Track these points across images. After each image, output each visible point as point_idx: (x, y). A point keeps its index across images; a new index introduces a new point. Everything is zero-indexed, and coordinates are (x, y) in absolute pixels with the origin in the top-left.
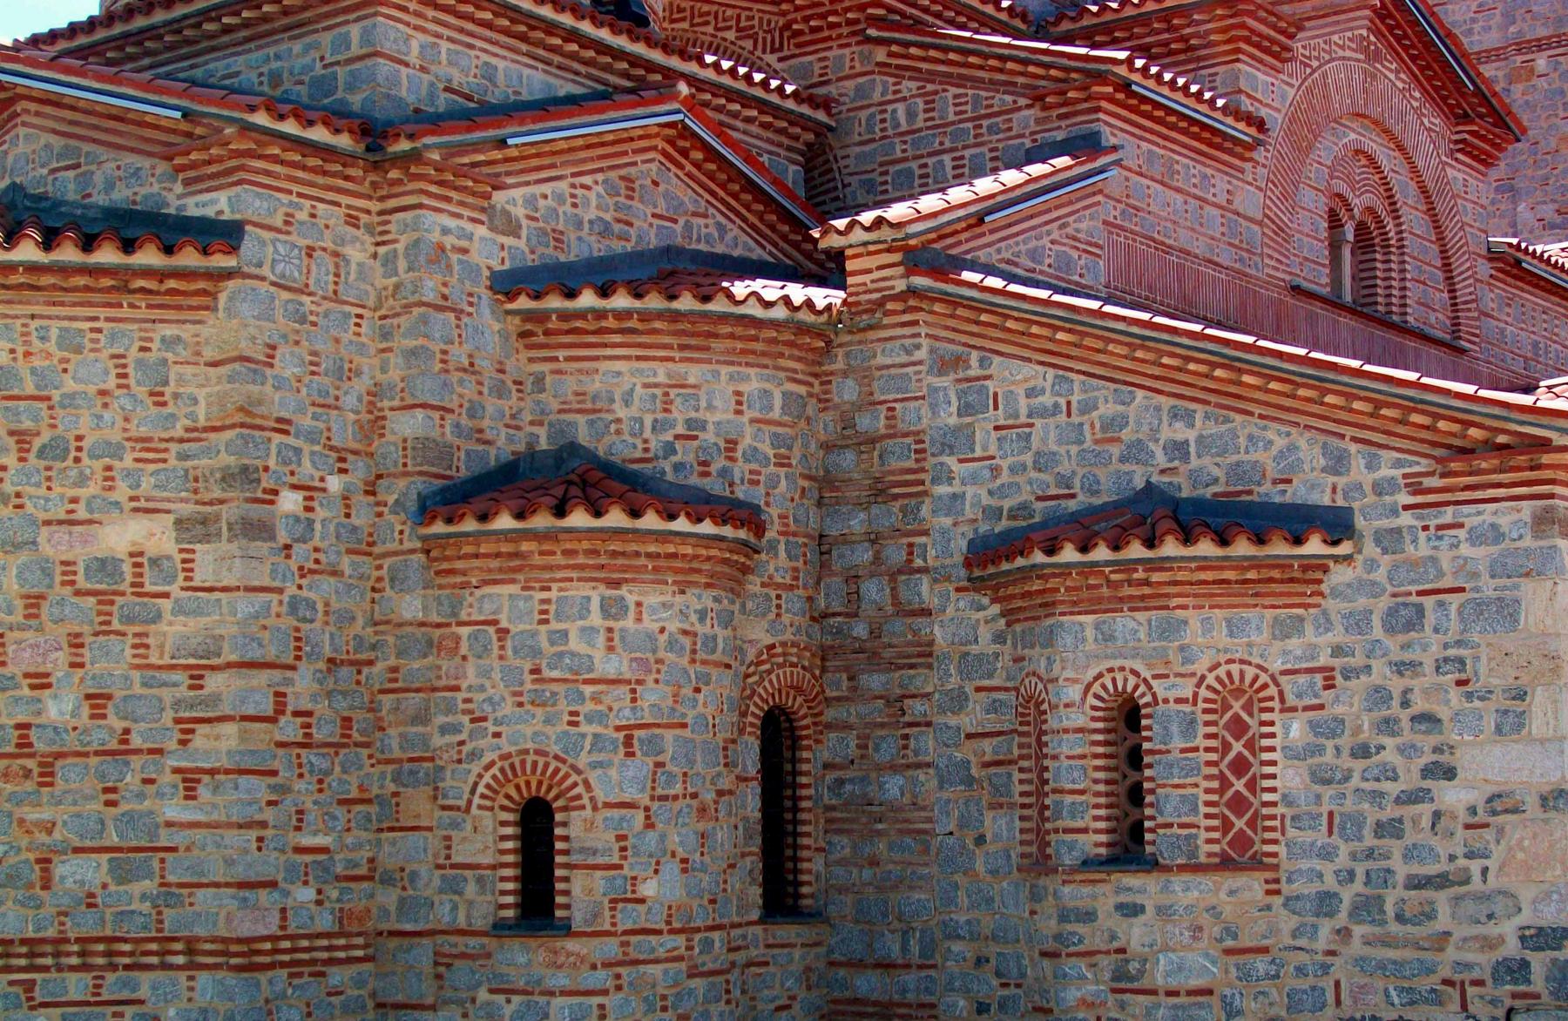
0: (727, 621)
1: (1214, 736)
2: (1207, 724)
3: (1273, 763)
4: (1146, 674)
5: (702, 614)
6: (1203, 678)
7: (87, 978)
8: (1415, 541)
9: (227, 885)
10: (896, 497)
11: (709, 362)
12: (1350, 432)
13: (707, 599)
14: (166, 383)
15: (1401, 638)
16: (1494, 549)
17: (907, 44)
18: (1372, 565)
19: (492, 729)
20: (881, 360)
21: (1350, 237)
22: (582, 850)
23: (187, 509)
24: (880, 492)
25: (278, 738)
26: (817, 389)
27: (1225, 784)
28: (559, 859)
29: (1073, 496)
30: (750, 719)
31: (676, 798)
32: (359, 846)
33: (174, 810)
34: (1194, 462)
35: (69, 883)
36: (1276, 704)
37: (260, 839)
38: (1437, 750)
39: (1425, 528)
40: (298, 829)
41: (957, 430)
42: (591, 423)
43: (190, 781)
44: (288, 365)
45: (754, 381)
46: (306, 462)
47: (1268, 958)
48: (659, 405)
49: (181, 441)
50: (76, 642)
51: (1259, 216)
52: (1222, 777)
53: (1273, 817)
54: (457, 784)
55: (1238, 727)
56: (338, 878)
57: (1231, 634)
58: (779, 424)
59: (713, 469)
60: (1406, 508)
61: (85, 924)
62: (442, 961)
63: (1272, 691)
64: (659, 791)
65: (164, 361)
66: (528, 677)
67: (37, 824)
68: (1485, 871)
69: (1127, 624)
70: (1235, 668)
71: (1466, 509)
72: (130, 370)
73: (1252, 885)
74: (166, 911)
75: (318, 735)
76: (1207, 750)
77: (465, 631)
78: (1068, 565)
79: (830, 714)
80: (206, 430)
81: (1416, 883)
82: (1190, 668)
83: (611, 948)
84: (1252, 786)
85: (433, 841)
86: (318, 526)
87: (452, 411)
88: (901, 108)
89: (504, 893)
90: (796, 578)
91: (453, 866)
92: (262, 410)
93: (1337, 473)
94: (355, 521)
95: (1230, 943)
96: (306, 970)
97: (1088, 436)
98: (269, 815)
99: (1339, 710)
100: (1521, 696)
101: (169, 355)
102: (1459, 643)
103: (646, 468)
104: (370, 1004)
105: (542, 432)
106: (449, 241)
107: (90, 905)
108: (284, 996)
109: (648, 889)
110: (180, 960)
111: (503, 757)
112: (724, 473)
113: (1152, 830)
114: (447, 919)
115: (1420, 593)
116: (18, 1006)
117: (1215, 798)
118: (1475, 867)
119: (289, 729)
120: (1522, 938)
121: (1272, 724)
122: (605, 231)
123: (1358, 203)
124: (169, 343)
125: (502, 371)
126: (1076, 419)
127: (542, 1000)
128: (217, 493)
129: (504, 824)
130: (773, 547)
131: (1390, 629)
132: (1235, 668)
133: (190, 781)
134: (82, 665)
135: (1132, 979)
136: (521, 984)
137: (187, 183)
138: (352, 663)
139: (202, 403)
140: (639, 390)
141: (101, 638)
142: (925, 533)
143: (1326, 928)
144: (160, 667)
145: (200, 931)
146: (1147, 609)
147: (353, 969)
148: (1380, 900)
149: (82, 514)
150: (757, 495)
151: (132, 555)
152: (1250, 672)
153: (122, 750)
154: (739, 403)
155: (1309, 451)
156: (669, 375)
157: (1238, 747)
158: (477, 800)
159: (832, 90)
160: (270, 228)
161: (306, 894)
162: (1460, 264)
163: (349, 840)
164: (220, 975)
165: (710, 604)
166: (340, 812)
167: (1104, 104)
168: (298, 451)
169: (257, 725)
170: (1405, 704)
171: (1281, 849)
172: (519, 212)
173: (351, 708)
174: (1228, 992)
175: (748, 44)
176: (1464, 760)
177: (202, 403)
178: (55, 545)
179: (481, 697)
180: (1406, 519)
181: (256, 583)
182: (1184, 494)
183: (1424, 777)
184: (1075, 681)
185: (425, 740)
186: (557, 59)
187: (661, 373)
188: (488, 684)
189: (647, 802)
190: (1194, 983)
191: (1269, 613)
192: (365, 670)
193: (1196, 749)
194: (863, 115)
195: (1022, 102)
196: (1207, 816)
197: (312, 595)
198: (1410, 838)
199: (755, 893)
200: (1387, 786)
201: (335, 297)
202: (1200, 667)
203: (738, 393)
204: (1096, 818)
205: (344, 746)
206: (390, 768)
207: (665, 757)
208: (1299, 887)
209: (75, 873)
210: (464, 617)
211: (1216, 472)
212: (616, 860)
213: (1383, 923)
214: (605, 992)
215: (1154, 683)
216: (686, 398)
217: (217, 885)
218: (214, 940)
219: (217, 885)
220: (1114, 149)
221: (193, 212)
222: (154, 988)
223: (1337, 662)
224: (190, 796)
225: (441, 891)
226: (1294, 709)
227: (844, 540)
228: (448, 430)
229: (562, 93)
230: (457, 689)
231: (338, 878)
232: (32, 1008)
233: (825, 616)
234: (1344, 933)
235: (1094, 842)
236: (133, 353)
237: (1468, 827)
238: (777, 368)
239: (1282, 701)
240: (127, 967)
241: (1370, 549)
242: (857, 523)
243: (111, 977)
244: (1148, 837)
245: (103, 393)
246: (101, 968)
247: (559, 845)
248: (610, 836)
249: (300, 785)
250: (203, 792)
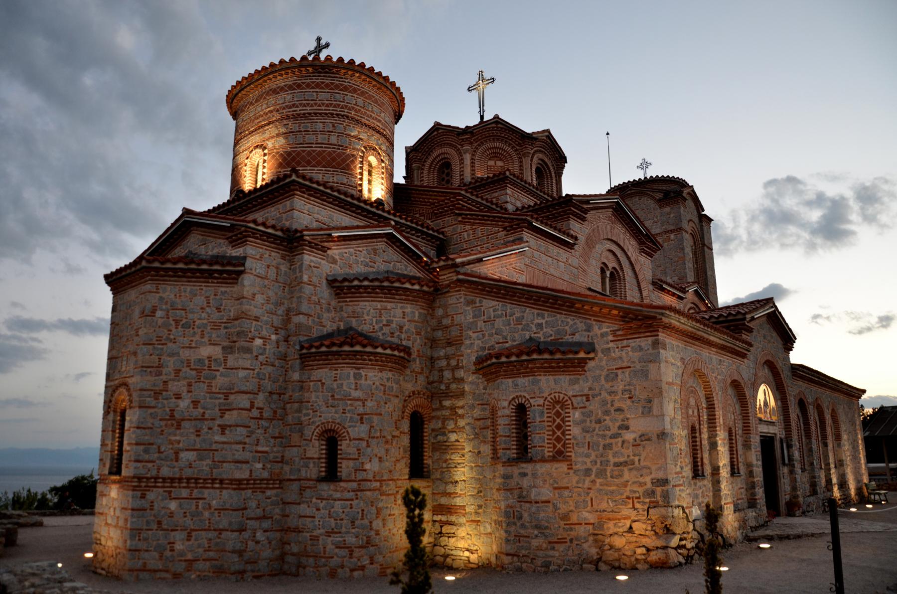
0: (398, 382)
1: (550, 417)
2: (548, 413)
3: (570, 426)
4: (528, 397)
5: (388, 379)
6: (546, 398)
7: (188, 491)
8: (614, 352)
9: (232, 462)
10: (454, 345)
11: (394, 302)
12: (593, 318)
13: (390, 374)
14: (221, 305)
15: (610, 384)
16: (640, 354)
17: (466, 215)
18: (601, 360)
19: (319, 414)
20: (450, 302)
21: (608, 275)
22: (345, 453)
23: (226, 344)
24: (450, 344)
25: (251, 416)
26: (431, 311)
27: (554, 433)
28: (339, 456)
29: (507, 342)
30: (406, 414)
31: (377, 437)
32: (278, 452)
33: (218, 438)
34: (545, 330)
35: (184, 460)
36: (570, 406)
37: (244, 448)
38: (623, 421)
39: (618, 348)
40: (257, 445)
41: (473, 322)
42: (357, 321)
43: (223, 428)
44: (260, 299)
45: (409, 309)
46: (264, 330)
47: (568, 491)
48: (378, 316)
49: (225, 323)
50: (190, 385)
51: (577, 266)
52: (553, 431)
53: (570, 444)
54: (308, 432)
55: (558, 414)
56: (270, 461)
57: (555, 384)
58: (417, 322)
59: (395, 335)
60: (611, 341)
61: (188, 473)
62: (302, 489)
63: (569, 402)
64: (372, 435)
65: (221, 299)
66: (330, 398)
67: (175, 441)
68: (639, 460)
69: (522, 381)
70: (557, 395)
71: (630, 341)
72: (211, 301)
73: (563, 467)
74: (214, 470)
75: (265, 415)
76: (548, 421)
77: (312, 384)
78: (503, 363)
79: (434, 414)
80: (233, 320)
81: (617, 465)
82: (543, 395)
84: (563, 433)
85: (301, 450)
86: (267, 350)
87: (311, 316)
88: (465, 234)
89: (321, 467)
90: (422, 370)
91: (307, 458)
92: (250, 313)
93: (589, 331)
94: (280, 349)
95: (556, 485)
96: (259, 490)
97: (512, 322)
98: (247, 440)
99: (591, 407)
100: (650, 401)
101: (223, 298)
102: (629, 385)
103: (373, 335)
104: (280, 502)
105: (342, 324)
106: (312, 264)
107: (190, 467)
108: (250, 498)
110: (217, 486)
111: (322, 424)
112: (398, 336)
113: (530, 448)
114: (304, 475)
115: (617, 369)
116: (166, 499)
117: (551, 437)
118: (636, 459)
119: (255, 413)
120: (652, 483)
121: (569, 413)
123: (610, 266)
125: (330, 305)
126: (508, 318)
127: (332, 502)
128: (235, 339)
129: (322, 445)
130: (414, 360)
131: (607, 381)
132: (557, 395)
133: (223, 428)
134: (191, 392)
135: (524, 498)
136: (325, 497)
137: (233, 247)
138: (277, 394)
139: (232, 311)
140: (372, 311)
141: (198, 383)
142: (463, 356)
143: (588, 480)
144: (215, 393)
145: (224, 476)
146: (529, 376)
147: (274, 491)
148: (605, 470)
149: (193, 345)
150: (409, 344)
151: (208, 358)
152: (562, 396)
153: (203, 418)
154: (404, 315)
155: (580, 325)
156: (381, 306)
157: (558, 421)
158: (314, 437)
159: (446, 229)
160: (255, 259)
161: (260, 466)
162: (643, 285)
163: (275, 449)
164: (229, 491)
165: (391, 376)
166: (272, 440)
167: (525, 229)
168: (261, 327)
169: (244, 412)
170: (612, 405)
171: (573, 454)
172: (337, 257)
173: (277, 407)
174: (555, 502)
175: (422, 218)
176: (631, 423)
177: (232, 311)
179: (315, 405)
180: (611, 345)
181: (245, 367)
182: (542, 340)
183: (619, 429)
184: (506, 400)
185: (299, 418)
186: (354, 215)
187: (379, 305)
188: (318, 400)
189: (367, 438)
190: (544, 499)
191: (568, 377)
192: (282, 396)
193: (544, 421)
194: (455, 236)
195: (501, 229)
196: (548, 443)
197: (265, 372)
198: (615, 449)
199: (407, 470)
200: (607, 432)
201: (277, 281)
202: (546, 395)
203: (404, 312)
204: (513, 445)
205: (274, 419)
206: (288, 427)
207: (374, 424)
208: (579, 466)
209: (187, 456)
210: (312, 379)
211: (551, 332)
212: (356, 457)
213: (606, 478)
214: (352, 500)
215: (531, 400)
216: (387, 313)
217: (230, 462)
218: (228, 480)
219: (230, 462)
220: (527, 242)
221: (234, 254)
222: (209, 494)
223: (590, 393)
224: (223, 433)
225: (303, 467)
226: (576, 408)
227: (439, 358)
228: (310, 322)
229: (355, 224)
230: (309, 402)
231: (270, 461)
232: (171, 499)
233: (433, 382)
234: (593, 482)
235: (513, 453)
236: (212, 297)
237: (633, 446)
238: (416, 305)
239: (573, 405)
240: (201, 487)
241: (600, 355)
242: (442, 353)
243: (196, 491)
244: (529, 450)
245: (202, 308)
246: (193, 487)
247: (339, 452)
248: (355, 449)
249: (259, 431)
250: (227, 432)
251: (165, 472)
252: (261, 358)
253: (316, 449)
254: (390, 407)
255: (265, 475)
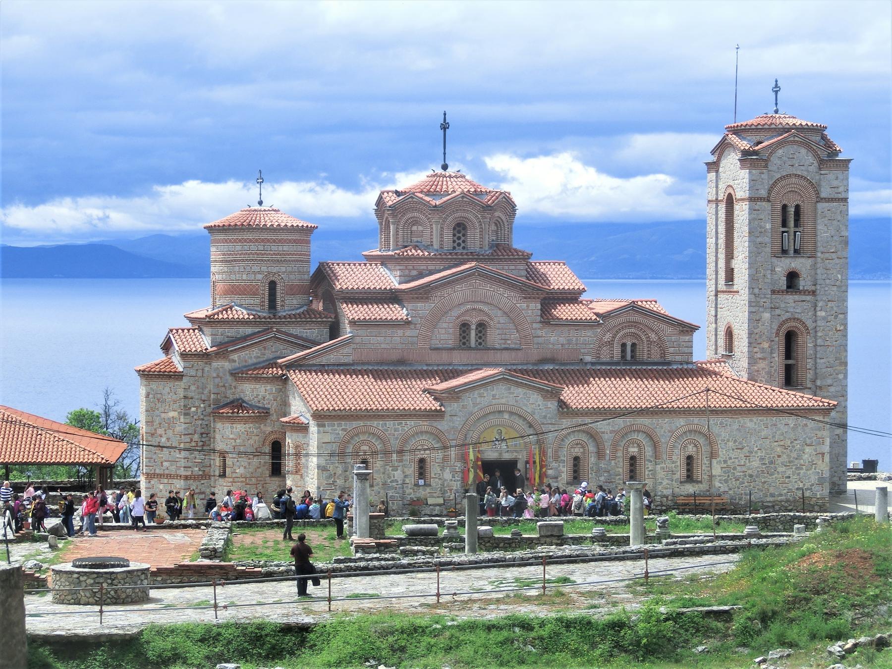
13: (251, 425)
44: (193, 388)
45: (269, 387)
61: (167, 472)
83: (231, 480)
109: (238, 471)
122: (259, 357)
124: (177, 385)
130: (272, 414)
150: (269, 406)
161: (197, 469)
178: (163, 415)
251: (157, 471)
252: (195, 417)
253: (218, 461)
254: (251, 442)
255: (201, 473)
